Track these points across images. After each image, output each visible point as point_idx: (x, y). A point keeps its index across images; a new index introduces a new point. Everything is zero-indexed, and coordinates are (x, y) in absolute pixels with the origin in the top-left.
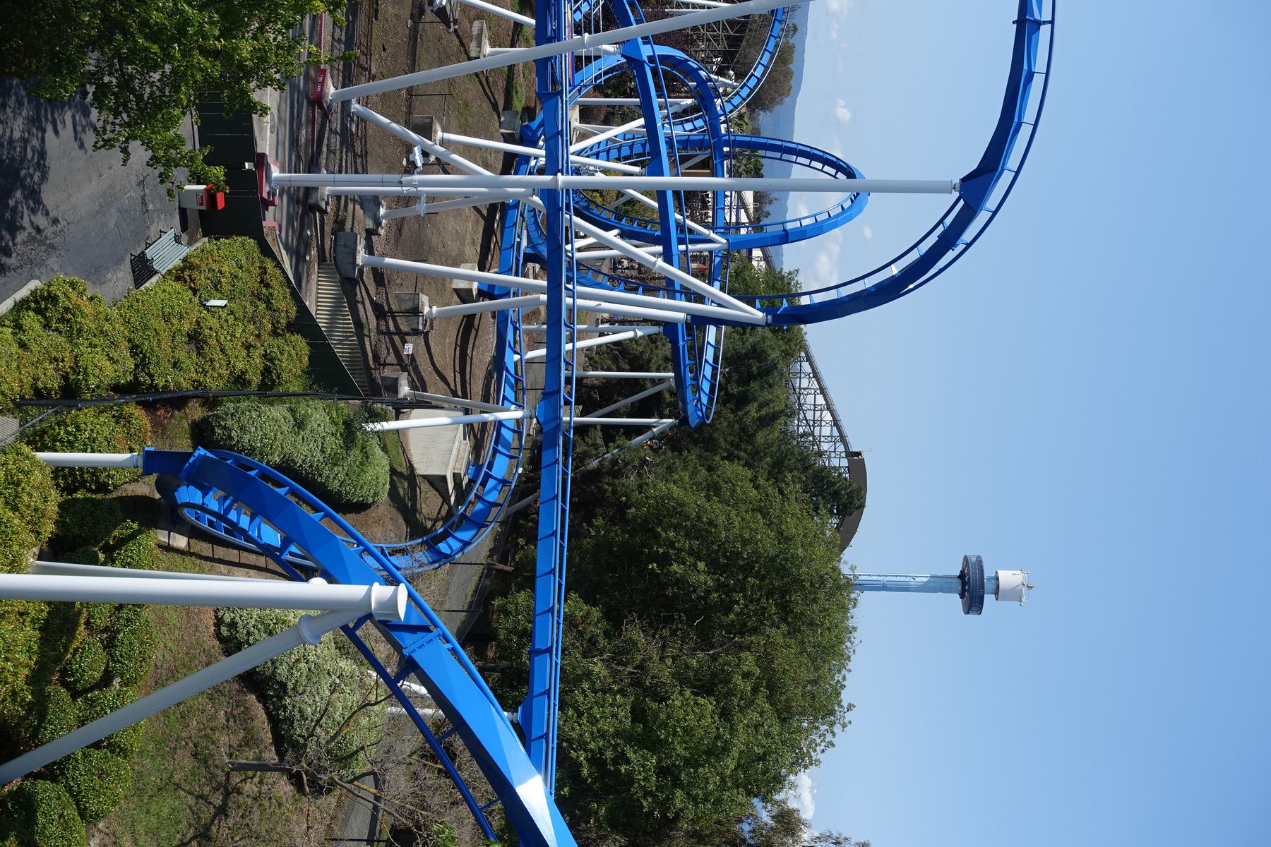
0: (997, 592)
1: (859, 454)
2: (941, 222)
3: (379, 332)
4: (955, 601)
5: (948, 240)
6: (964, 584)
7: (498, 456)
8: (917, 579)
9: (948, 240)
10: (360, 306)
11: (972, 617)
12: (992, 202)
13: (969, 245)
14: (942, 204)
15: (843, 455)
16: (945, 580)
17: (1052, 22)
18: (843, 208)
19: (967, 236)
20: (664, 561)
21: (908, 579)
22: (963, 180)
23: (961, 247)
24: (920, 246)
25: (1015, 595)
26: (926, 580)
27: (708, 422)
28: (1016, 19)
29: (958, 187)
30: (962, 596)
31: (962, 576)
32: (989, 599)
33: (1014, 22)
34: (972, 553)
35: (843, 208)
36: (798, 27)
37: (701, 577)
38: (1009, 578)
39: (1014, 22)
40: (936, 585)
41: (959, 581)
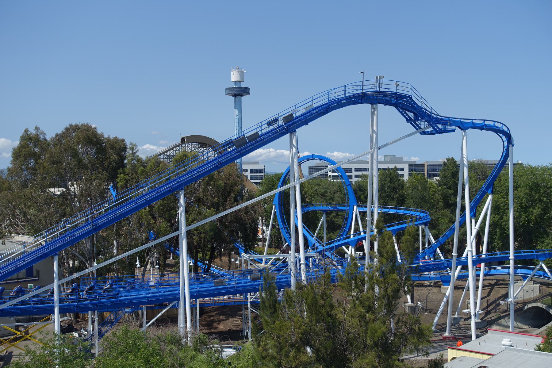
0: (240, 82)
1: (183, 139)
3: (496, 312)
4: (244, 98)
6: (239, 95)
8: (237, 114)
10: (492, 318)
11: (251, 91)
16: (237, 104)
20: (529, 221)
21: (237, 118)
25: (242, 74)
26: (237, 111)
30: (242, 96)
31: (235, 96)
32: (243, 85)
34: (224, 92)
37: (537, 210)
38: (234, 76)
40: (238, 106)
41: (237, 97)
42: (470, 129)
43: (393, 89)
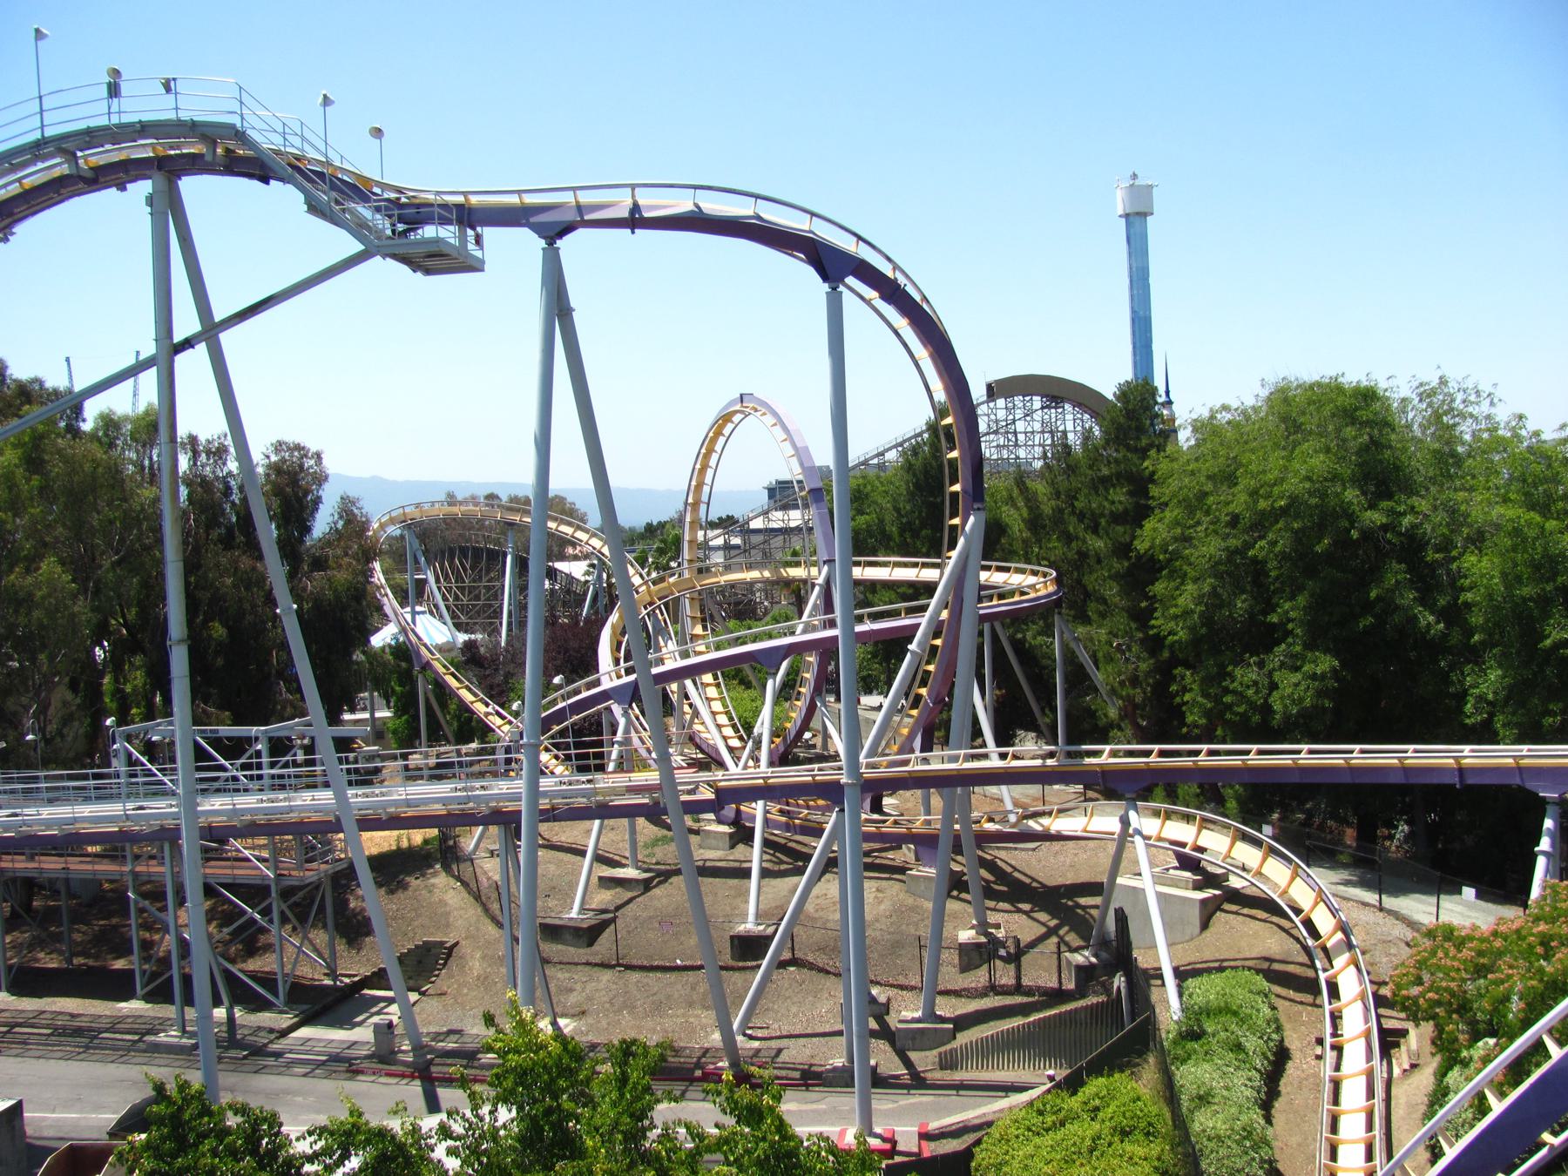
1: (989, 387)
2: (868, 302)
5: (892, 292)
7: (1163, 835)
9: (892, 292)
12: (847, 244)
13: (896, 267)
14: (857, 300)
15: (992, 405)
17: (633, 187)
18: (775, 425)
19: (887, 270)
22: (825, 278)
23: (902, 280)
24: (896, 326)
27: (1054, 574)
28: (629, 231)
29: (834, 285)
33: (633, 233)
35: (775, 425)
36: (489, 492)
39: (633, 233)
42: (581, 234)
43: (159, 109)
